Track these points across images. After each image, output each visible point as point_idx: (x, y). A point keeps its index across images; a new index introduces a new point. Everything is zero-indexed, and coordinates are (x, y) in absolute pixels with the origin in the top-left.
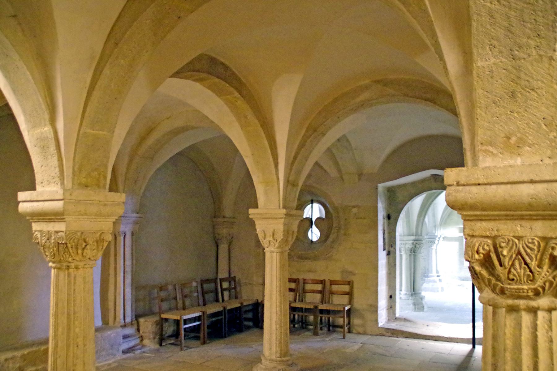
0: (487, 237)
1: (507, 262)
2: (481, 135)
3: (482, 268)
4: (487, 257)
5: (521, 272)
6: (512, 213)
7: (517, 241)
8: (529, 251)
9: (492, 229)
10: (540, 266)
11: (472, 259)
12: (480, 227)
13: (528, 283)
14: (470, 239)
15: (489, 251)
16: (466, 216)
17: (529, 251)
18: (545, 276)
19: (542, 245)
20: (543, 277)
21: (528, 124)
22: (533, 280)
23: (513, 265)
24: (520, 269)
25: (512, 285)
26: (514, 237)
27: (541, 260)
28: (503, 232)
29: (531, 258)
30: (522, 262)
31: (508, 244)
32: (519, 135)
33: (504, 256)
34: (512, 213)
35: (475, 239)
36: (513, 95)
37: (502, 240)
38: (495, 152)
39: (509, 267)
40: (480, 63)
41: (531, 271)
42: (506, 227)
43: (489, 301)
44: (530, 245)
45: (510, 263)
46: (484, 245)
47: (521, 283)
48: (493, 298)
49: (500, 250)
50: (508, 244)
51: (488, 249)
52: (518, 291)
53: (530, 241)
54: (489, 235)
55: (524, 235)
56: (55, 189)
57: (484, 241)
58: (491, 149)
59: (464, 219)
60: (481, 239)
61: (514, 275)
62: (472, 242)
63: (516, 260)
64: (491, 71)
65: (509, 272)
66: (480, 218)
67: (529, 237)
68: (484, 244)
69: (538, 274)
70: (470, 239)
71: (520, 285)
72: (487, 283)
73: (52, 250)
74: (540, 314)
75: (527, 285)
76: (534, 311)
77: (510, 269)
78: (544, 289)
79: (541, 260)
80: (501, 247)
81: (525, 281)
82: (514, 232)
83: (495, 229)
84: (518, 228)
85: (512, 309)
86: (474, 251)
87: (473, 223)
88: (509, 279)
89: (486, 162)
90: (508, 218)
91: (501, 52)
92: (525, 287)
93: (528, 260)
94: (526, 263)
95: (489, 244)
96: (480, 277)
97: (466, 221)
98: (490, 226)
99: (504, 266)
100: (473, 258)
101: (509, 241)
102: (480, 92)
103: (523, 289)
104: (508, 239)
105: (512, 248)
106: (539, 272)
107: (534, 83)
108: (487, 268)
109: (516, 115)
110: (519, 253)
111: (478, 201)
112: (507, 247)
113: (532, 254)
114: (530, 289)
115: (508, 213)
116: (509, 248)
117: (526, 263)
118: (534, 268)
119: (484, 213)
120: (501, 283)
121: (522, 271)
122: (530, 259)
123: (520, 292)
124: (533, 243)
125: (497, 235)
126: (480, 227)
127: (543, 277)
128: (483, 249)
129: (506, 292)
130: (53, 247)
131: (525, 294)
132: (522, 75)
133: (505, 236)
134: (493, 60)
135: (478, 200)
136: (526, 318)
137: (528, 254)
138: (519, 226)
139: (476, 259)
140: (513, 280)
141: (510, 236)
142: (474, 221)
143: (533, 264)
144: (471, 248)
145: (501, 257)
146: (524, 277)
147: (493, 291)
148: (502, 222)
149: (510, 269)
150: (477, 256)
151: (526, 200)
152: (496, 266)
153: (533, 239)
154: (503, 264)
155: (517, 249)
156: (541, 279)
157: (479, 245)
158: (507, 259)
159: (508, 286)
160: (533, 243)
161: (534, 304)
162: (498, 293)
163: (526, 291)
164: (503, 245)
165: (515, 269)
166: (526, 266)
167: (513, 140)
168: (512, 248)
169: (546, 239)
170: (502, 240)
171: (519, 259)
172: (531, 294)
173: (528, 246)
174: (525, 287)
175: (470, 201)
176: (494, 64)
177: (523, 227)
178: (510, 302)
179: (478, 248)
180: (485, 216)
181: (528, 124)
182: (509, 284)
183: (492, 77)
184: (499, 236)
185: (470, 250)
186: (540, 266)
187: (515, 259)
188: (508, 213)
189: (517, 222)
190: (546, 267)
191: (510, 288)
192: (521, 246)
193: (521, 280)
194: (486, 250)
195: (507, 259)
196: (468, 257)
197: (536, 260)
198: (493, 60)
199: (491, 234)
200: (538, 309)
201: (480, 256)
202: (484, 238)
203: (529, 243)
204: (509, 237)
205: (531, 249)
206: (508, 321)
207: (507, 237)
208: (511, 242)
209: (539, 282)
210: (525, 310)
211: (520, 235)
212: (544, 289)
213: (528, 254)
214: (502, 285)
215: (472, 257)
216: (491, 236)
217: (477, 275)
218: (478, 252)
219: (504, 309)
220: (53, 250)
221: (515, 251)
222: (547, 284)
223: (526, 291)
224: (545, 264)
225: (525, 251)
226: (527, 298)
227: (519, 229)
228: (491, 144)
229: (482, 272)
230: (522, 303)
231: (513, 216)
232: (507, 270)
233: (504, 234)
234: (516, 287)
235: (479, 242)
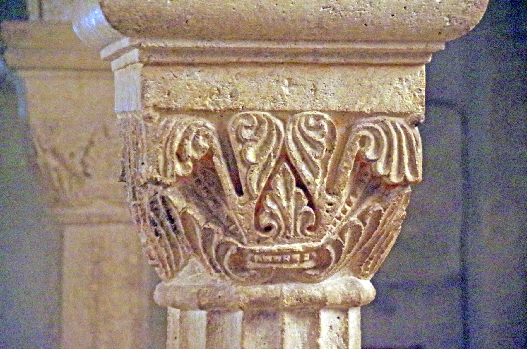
0: (206, 113)
3: (188, 201)
5: (288, 206)
6: (273, 46)
8: (308, 149)
9: (218, 90)
11: (166, 176)
12: (189, 85)
13: (306, 235)
14: (160, 120)
15: (210, 155)
16: (154, 50)
17: (308, 149)
18: (344, 216)
20: (339, 218)
23: (268, 187)
24: (288, 199)
25: (266, 244)
26: (273, 112)
27: (336, 172)
28: (246, 99)
30: (292, 181)
31: (258, 130)
33: (248, 165)
34: (273, 46)
37: (245, 122)
39: (257, 193)
42: (254, 84)
44: (311, 134)
45: (263, 185)
46: (196, 137)
47: (288, 238)
49: (237, 148)
50: (258, 130)
51: (208, 146)
52: (279, 258)
53: (312, 122)
54: (212, 108)
55: (298, 108)
57: (196, 125)
59: (145, 59)
60: (189, 119)
61: (272, 215)
62: (165, 127)
63: (278, 175)
65: (259, 209)
66: (189, 59)
67: (310, 113)
68: (198, 132)
69: (327, 211)
70: (160, 120)
71: (284, 243)
75: (301, 241)
77: (262, 198)
79: (336, 172)
80: (239, 140)
81: (298, 230)
82: (275, 100)
83: (227, 91)
84: (283, 88)
86: (171, 152)
87: (167, 74)
88: (258, 226)
90: (261, 59)
92: (298, 247)
93: (307, 175)
94: (300, 184)
95: (211, 133)
96: (181, 229)
97: (148, 68)
98: (213, 83)
99: (248, 190)
100: (169, 173)
101: (261, 123)
103: (293, 252)
104: (258, 117)
105: (267, 142)
106: (330, 204)
108: (200, 201)
110: (285, 157)
111: (192, 10)
112: (256, 141)
113: (316, 157)
114: (308, 250)
115: (264, 45)
116: (260, 142)
117: (300, 184)
118: (320, 194)
119: (200, 44)
120: (237, 240)
121: (292, 202)
122: (312, 172)
123: (282, 262)
124: (319, 128)
125: (231, 107)
126: (189, 85)
127: (339, 218)
128: (196, 146)
129: (250, 265)
131: (295, 266)
133: (251, 110)
135: (193, 7)
138: (286, 82)
139: (177, 176)
140: (268, 228)
141: (263, 110)
142: (171, 69)
144: (163, 145)
145: (240, 166)
146: (296, 220)
148: (245, 70)
149: (262, 198)
150: (178, 167)
152: (227, 192)
153: (318, 118)
154: (244, 188)
155: (280, 147)
156: (335, 224)
157: (186, 137)
159: (257, 248)
160: (319, 128)
162: (227, 267)
163: (297, 256)
164: (247, 134)
165: (275, 200)
166: (301, 191)
168: (267, 142)
170: (245, 122)
171: (285, 172)
173: (307, 139)
174: (298, 247)
177: (296, 85)
179: (181, 145)
180: (203, 52)
182: (259, 241)
184: (237, 110)
185: (161, 150)
187: (276, 171)
188: (264, 45)
189: (281, 71)
191: (262, 253)
192: (290, 137)
193: (287, 228)
194: (203, 149)
196: (155, 171)
197: (324, 176)
199: (218, 105)
201: (186, 167)
202: (198, 116)
203: (310, 128)
204: (261, 113)
205: (314, 144)
207: (256, 112)
208: (266, 127)
210: (291, 310)
214: (240, 245)
215: (165, 171)
216: (215, 110)
217: (172, 220)
221: (274, 151)
222: (347, 235)
223: (297, 256)
224: (344, 183)
225: (300, 150)
229: (190, 212)
231: (273, 53)
232: (254, 204)
233: (250, 105)
234: (275, 248)
235: (185, 127)
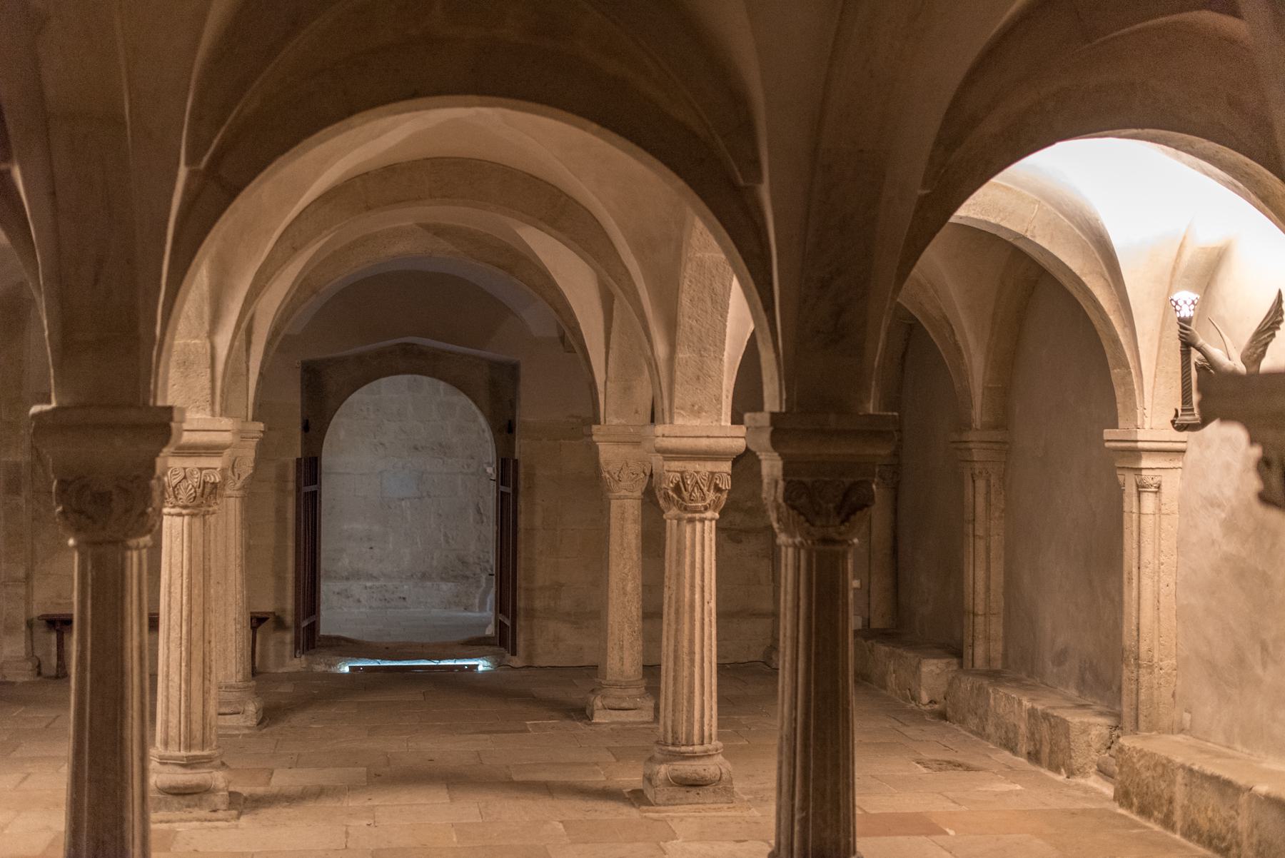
0: (678, 472)
1: (690, 488)
2: (677, 402)
4: (677, 485)
7: (696, 474)
10: (709, 490)
15: (678, 482)
19: (711, 476)
21: (705, 398)
22: (704, 499)
29: (704, 485)
31: (691, 476)
32: (700, 405)
33: (688, 485)
35: (670, 474)
36: (698, 378)
38: (684, 414)
40: (680, 355)
41: (703, 494)
43: (676, 516)
48: (678, 514)
49: (685, 480)
56: (204, 416)
58: (682, 412)
60: (674, 473)
64: (687, 362)
65: (691, 495)
72: (676, 503)
73: (193, 491)
74: (707, 522)
76: (702, 520)
78: (710, 505)
85: (691, 521)
87: (669, 462)
89: (679, 421)
91: (694, 351)
92: (700, 504)
93: (702, 487)
102: (678, 373)
107: (711, 373)
109: (699, 391)
110: (697, 482)
117: (701, 489)
124: (705, 476)
130: (195, 488)
132: (705, 367)
134: (688, 355)
136: (698, 525)
137: (702, 483)
143: (705, 489)
147: (679, 509)
150: (671, 485)
151: (704, 448)
158: (690, 487)
160: (705, 476)
161: (703, 515)
164: (688, 477)
167: (696, 407)
169: (713, 473)
172: (702, 509)
174: (700, 504)
175: (670, 447)
176: (689, 357)
178: (690, 515)
181: (705, 398)
183: (687, 365)
186: (709, 490)
190: (712, 491)
195: (690, 487)
198: (688, 355)
200: (706, 519)
205: (704, 479)
206: (688, 529)
209: (708, 501)
211: (699, 470)
212: (710, 505)
213: (702, 483)
218: (672, 482)
219: (685, 521)
220: (195, 492)
226: (700, 512)
227: (697, 466)
228: (682, 409)
230: (697, 516)
234: (694, 505)
